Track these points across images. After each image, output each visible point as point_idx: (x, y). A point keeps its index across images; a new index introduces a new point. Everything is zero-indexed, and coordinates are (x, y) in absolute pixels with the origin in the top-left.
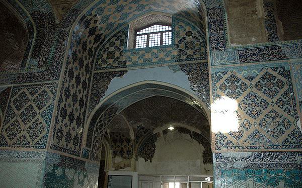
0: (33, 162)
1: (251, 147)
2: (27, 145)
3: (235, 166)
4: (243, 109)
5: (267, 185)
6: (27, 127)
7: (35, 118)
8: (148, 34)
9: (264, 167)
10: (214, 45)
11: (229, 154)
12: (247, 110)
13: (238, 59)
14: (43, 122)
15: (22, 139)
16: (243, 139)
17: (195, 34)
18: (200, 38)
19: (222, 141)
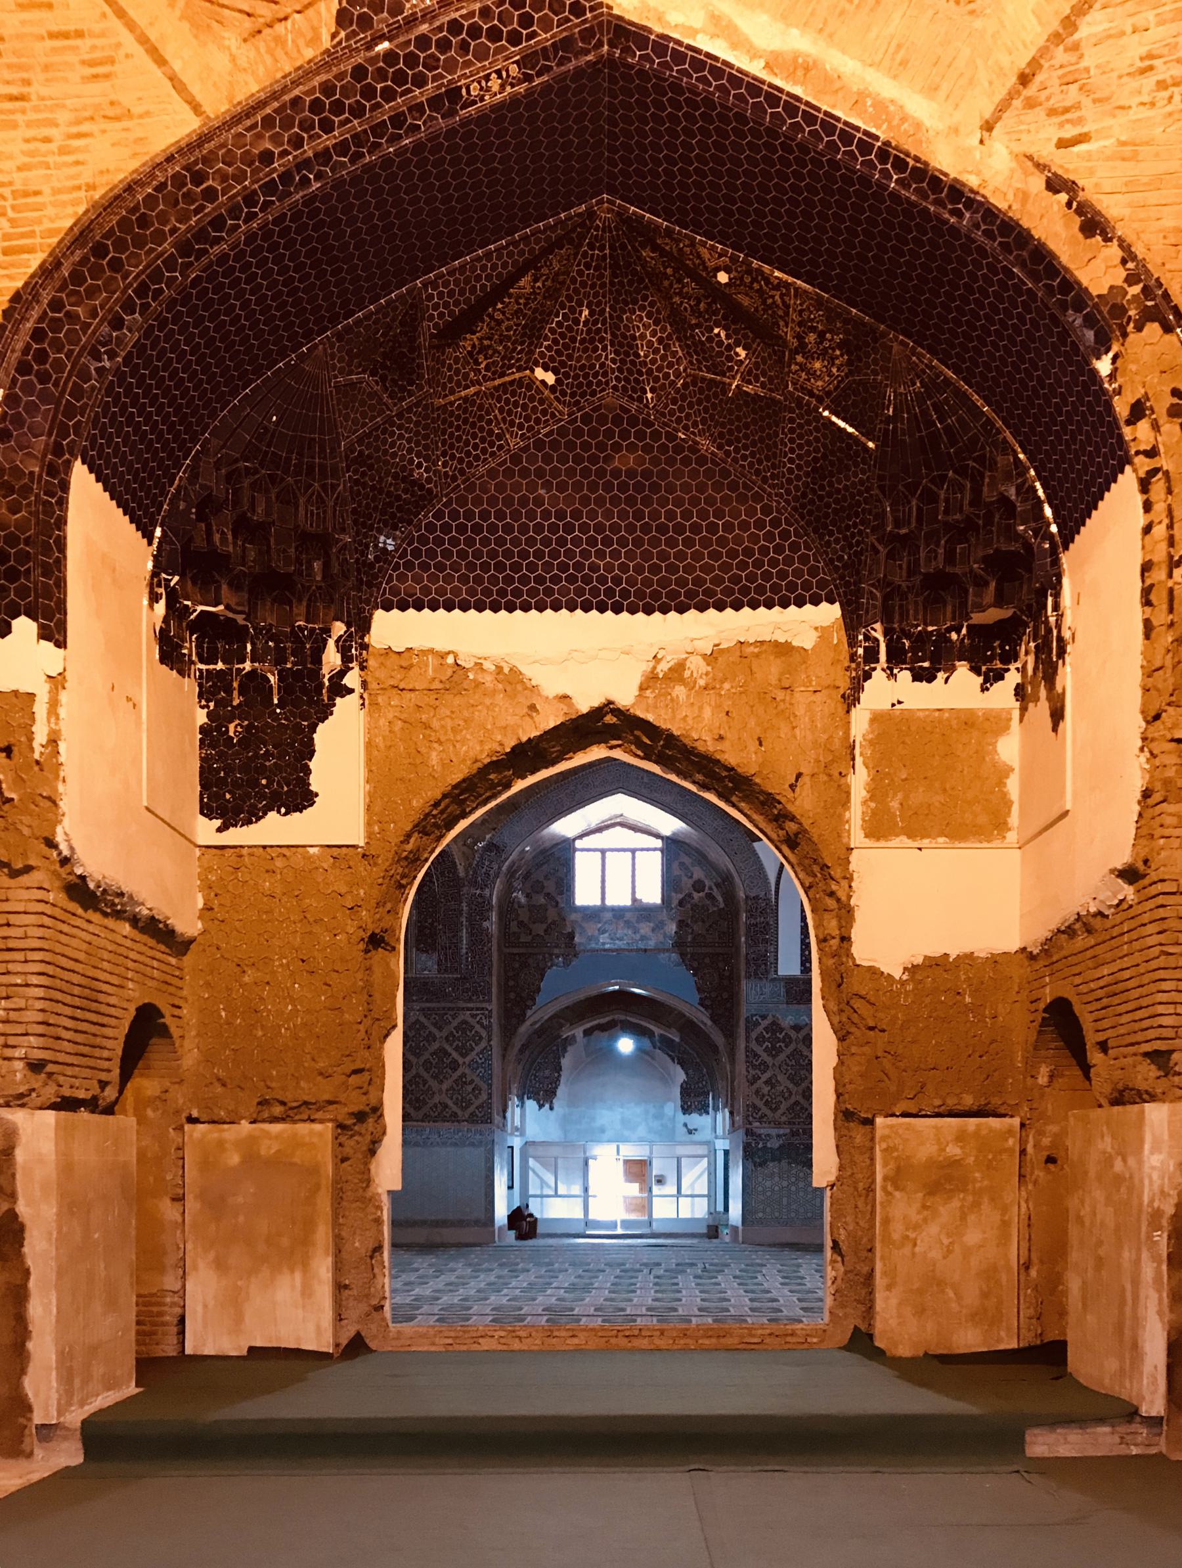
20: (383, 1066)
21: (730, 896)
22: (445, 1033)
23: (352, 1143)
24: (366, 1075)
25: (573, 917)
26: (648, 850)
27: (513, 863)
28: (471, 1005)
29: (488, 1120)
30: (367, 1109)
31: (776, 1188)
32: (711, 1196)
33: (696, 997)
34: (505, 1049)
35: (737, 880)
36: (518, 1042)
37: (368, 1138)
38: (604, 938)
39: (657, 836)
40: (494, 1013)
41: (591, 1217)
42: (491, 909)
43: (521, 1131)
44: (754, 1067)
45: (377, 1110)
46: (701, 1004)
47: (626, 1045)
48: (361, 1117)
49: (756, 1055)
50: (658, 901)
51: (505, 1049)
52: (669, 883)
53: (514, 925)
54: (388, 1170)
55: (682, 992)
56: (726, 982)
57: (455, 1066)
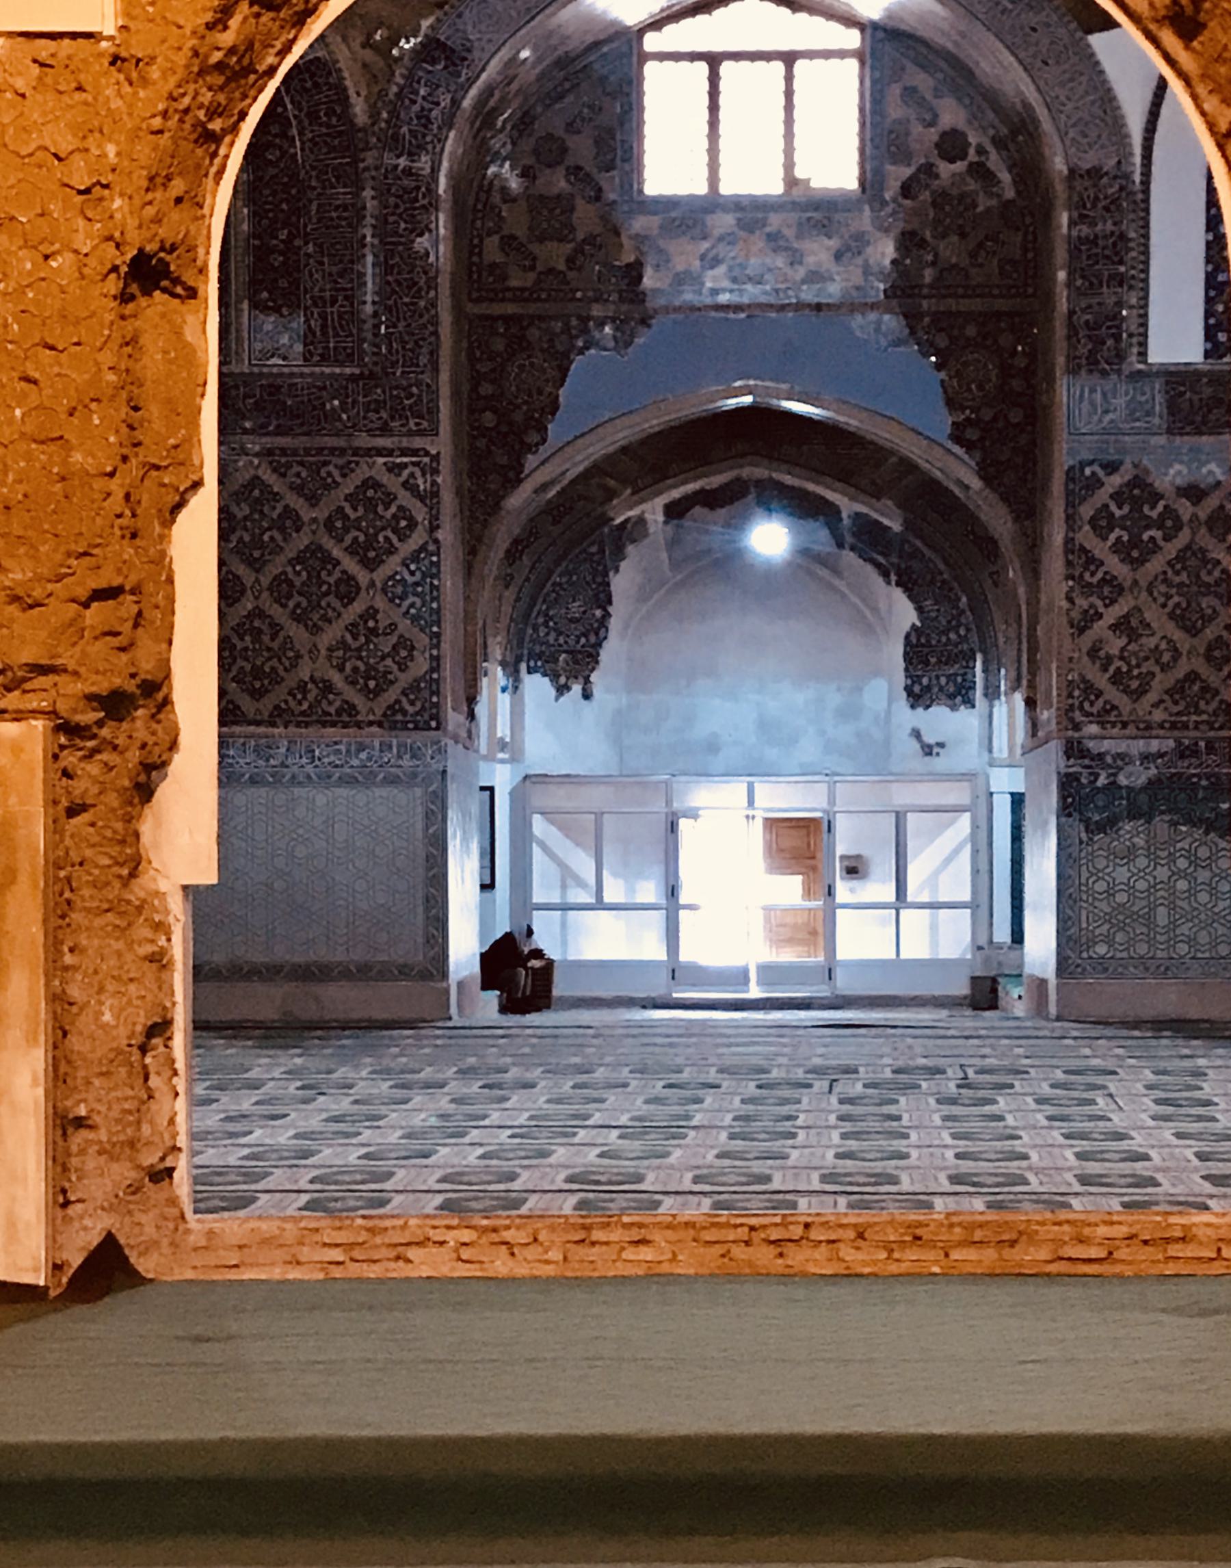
0: (392, 781)
1: (1174, 726)
2: (347, 717)
3: (1122, 780)
4: (1162, 600)
5: (1207, 833)
6: (327, 638)
7: (358, 607)
8: (714, 60)
9: (1204, 783)
10: (1083, 350)
11: (1106, 745)
12: (1171, 603)
13: (1161, 417)
14: (404, 625)
15: (313, 693)
16: (1152, 697)
17: (981, 151)
18: (1005, 177)
19: (1086, 705)
20: (170, 581)
21: (1029, 170)
22: (321, 513)
23: (93, 768)
24: (128, 605)
25: (639, 224)
26: (827, 54)
27: (489, 91)
28: (381, 442)
29: (431, 720)
30: (131, 686)
31: (1142, 885)
32: (980, 906)
33: (941, 422)
34: (473, 552)
35: (1047, 125)
36: (502, 535)
37: (134, 756)
38: (714, 278)
39: (849, 20)
40: (445, 464)
41: (685, 956)
42: (433, 205)
43: (511, 749)
44: (1088, 589)
45: (154, 691)
46: (957, 438)
47: (770, 538)
48: (115, 705)
49: (1092, 561)
50: (850, 182)
51: (472, 548)
52: (880, 139)
53: (492, 249)
54: (185, 835)
55: (909, 409)
56: (1016, 384)
57: (348, 590)
